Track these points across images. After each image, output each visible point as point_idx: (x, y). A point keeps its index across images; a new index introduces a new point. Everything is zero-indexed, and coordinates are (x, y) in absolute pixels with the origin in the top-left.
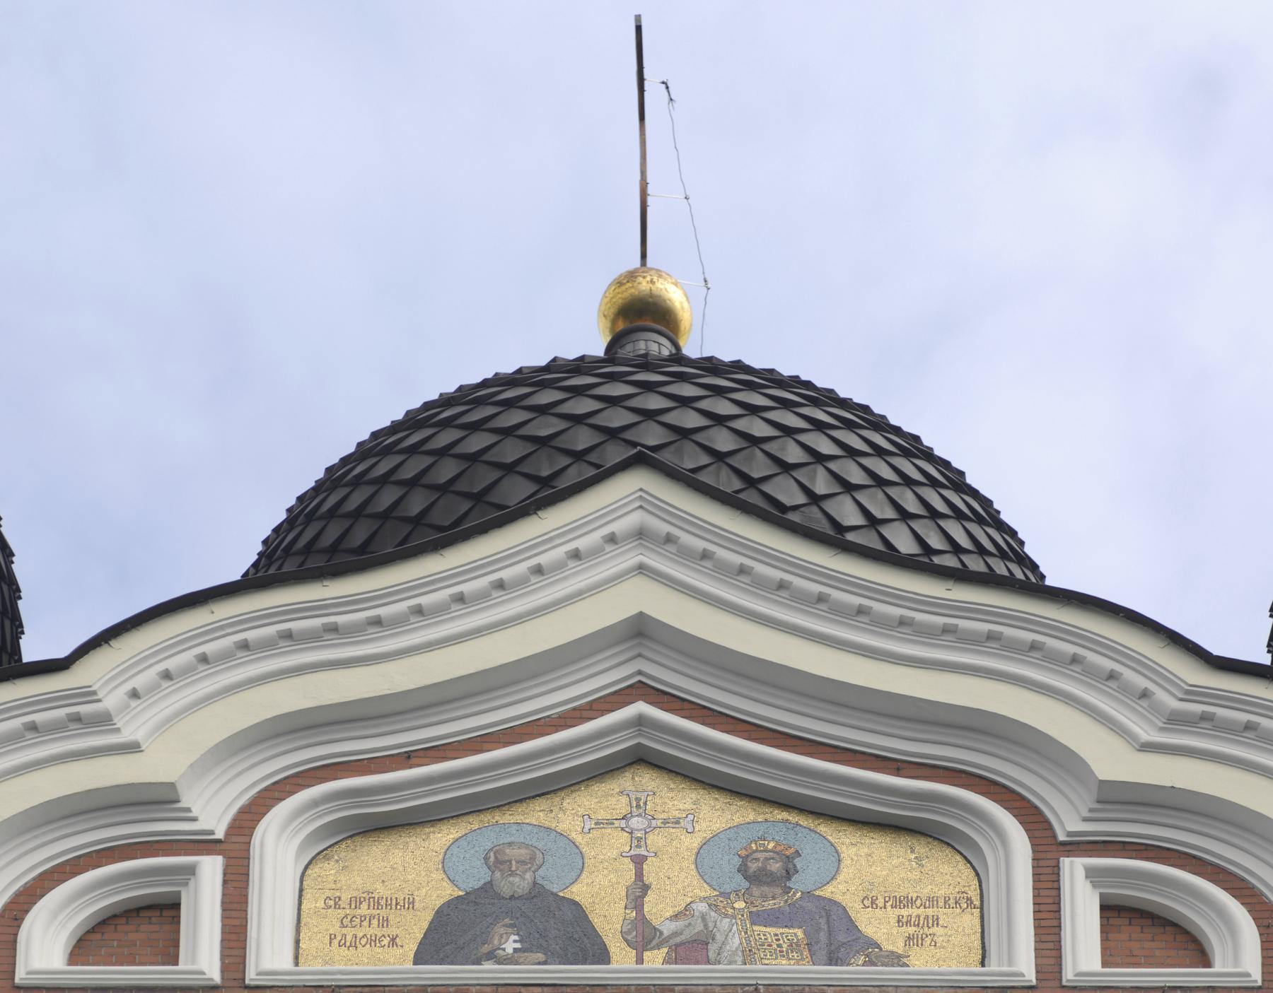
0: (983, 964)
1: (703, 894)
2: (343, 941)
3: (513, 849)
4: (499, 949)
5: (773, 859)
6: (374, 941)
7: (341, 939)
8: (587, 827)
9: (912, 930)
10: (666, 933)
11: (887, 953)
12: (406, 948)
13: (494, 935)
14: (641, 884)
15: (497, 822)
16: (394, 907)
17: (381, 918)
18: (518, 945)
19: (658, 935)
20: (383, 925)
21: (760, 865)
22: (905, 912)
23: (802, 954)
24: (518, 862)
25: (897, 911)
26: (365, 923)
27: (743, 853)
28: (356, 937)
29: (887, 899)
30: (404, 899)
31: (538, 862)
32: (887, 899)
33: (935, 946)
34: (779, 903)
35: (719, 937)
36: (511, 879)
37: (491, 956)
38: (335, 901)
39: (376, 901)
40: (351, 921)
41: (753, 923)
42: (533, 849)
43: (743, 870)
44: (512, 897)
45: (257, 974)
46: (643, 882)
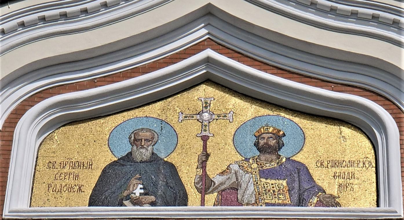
0: (378, 205)
1: (236, 160)
2: (55, 188)
3: (143, 132)
4: (132, 193)
6: (70, 189)
7: (54, 187)
8: (181, 118)
9: (341, 181)
11: (329, 196)
12: (86, 193)
13: (130, 185)
14: (206, 153)
15: (136, 116)
16: (82, 168)
17: (75, 174)
18: (142, 191)
19: (213, 185)
20: (75, 178)
21: (265, 141)
22: (338, 170)
23: (285, 197)
25: (334, 170)
26: (67, 177)
27: (257, 134)
28: (61, 186)
29: (329, 162)
30: (88, 162)
31: (155, 140)
33: (353, 191)
34: (274, 165)
35: (244, 186)
36: (141, 150)
37: (128, 198)
39: (73, 163)
40: (60, 176)
42: (153, 132)
43: (256, 144)
44: (141, 162)
45: (9, 212)
46: (206, 152)
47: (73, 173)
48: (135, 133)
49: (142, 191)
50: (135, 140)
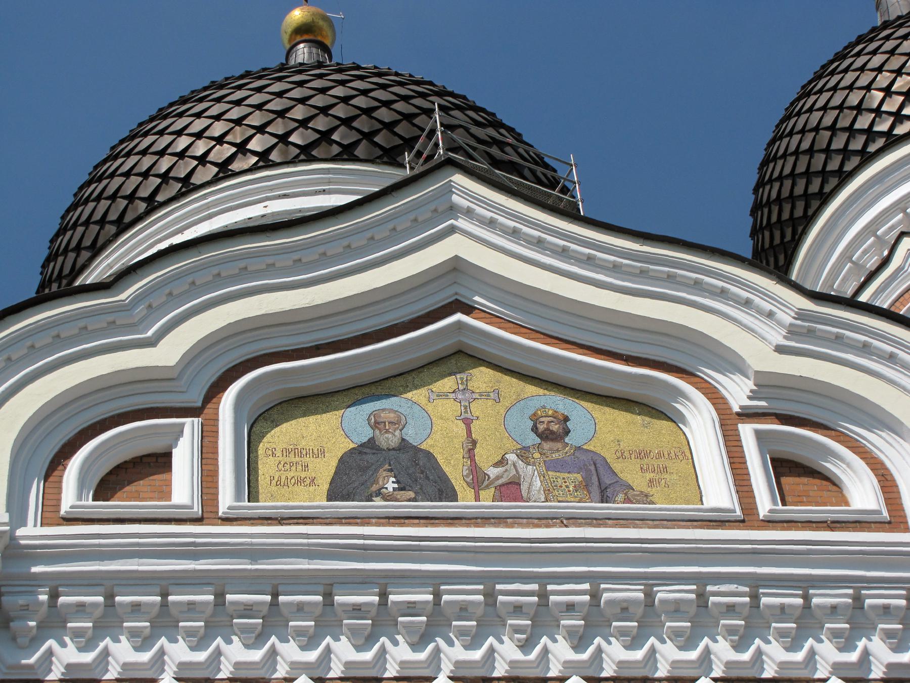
3: (386, 413)
4: (383, 488)
5: (552, 422)
10: (492, 476)
11: (638, 493)
13: (379, 478)
14: (471, 439)
15: (373, 394)
18: (396, 486)
19: (487, 478)
20: (305, 470)
21: (545, 426)
24: (389, 423)
29: (631, 452)
31: (402, 423)
32: (631, 452)
36: (386, 435)
37: (378, 493)
38: (272, 451)
39: (299, 451)
41: (548, 470)
43: (535, 429)
47: (300, 463)
48: (375, 414)
49: (396, 486)
50: (376, 422)
